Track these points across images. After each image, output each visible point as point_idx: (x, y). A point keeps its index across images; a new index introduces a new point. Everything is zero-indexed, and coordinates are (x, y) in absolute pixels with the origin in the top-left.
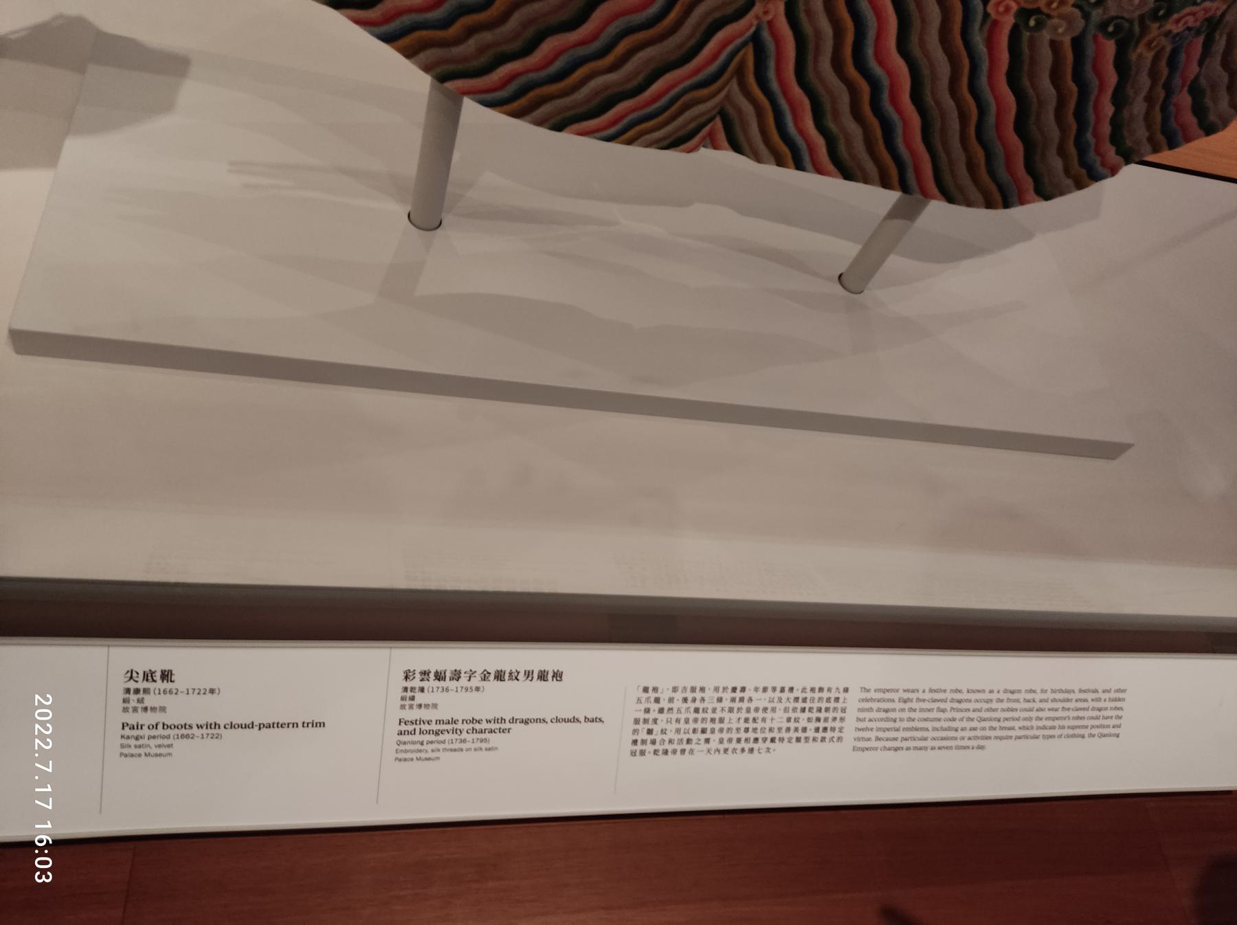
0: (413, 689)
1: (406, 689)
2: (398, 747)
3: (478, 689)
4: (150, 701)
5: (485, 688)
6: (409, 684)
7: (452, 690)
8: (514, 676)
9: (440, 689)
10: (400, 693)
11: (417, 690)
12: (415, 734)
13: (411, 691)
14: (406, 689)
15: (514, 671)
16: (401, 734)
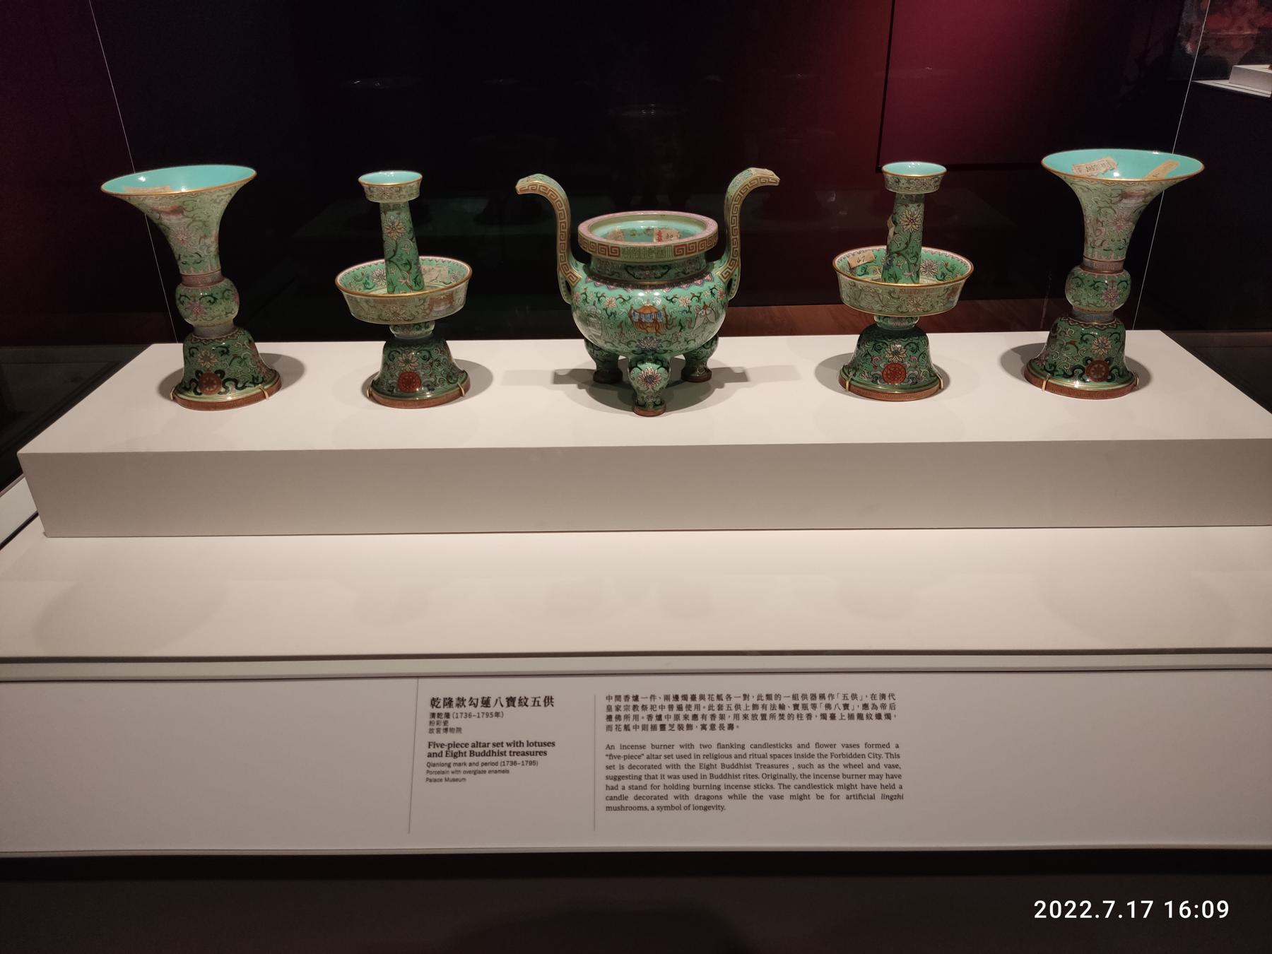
0: (439, 715)
1: (433, 715)
2: (428, 769)
3: (497, 714)
4: (452, 723)
5: (504, 713)
6: (436, 710)
7: (474, 716)
8: (523, 702)
9: (464, 715)
10: (428, 719)
12: (442, 756)
13: (438, 717)
14: (433, 715)
15: (523, 697)
16: (431, 756)
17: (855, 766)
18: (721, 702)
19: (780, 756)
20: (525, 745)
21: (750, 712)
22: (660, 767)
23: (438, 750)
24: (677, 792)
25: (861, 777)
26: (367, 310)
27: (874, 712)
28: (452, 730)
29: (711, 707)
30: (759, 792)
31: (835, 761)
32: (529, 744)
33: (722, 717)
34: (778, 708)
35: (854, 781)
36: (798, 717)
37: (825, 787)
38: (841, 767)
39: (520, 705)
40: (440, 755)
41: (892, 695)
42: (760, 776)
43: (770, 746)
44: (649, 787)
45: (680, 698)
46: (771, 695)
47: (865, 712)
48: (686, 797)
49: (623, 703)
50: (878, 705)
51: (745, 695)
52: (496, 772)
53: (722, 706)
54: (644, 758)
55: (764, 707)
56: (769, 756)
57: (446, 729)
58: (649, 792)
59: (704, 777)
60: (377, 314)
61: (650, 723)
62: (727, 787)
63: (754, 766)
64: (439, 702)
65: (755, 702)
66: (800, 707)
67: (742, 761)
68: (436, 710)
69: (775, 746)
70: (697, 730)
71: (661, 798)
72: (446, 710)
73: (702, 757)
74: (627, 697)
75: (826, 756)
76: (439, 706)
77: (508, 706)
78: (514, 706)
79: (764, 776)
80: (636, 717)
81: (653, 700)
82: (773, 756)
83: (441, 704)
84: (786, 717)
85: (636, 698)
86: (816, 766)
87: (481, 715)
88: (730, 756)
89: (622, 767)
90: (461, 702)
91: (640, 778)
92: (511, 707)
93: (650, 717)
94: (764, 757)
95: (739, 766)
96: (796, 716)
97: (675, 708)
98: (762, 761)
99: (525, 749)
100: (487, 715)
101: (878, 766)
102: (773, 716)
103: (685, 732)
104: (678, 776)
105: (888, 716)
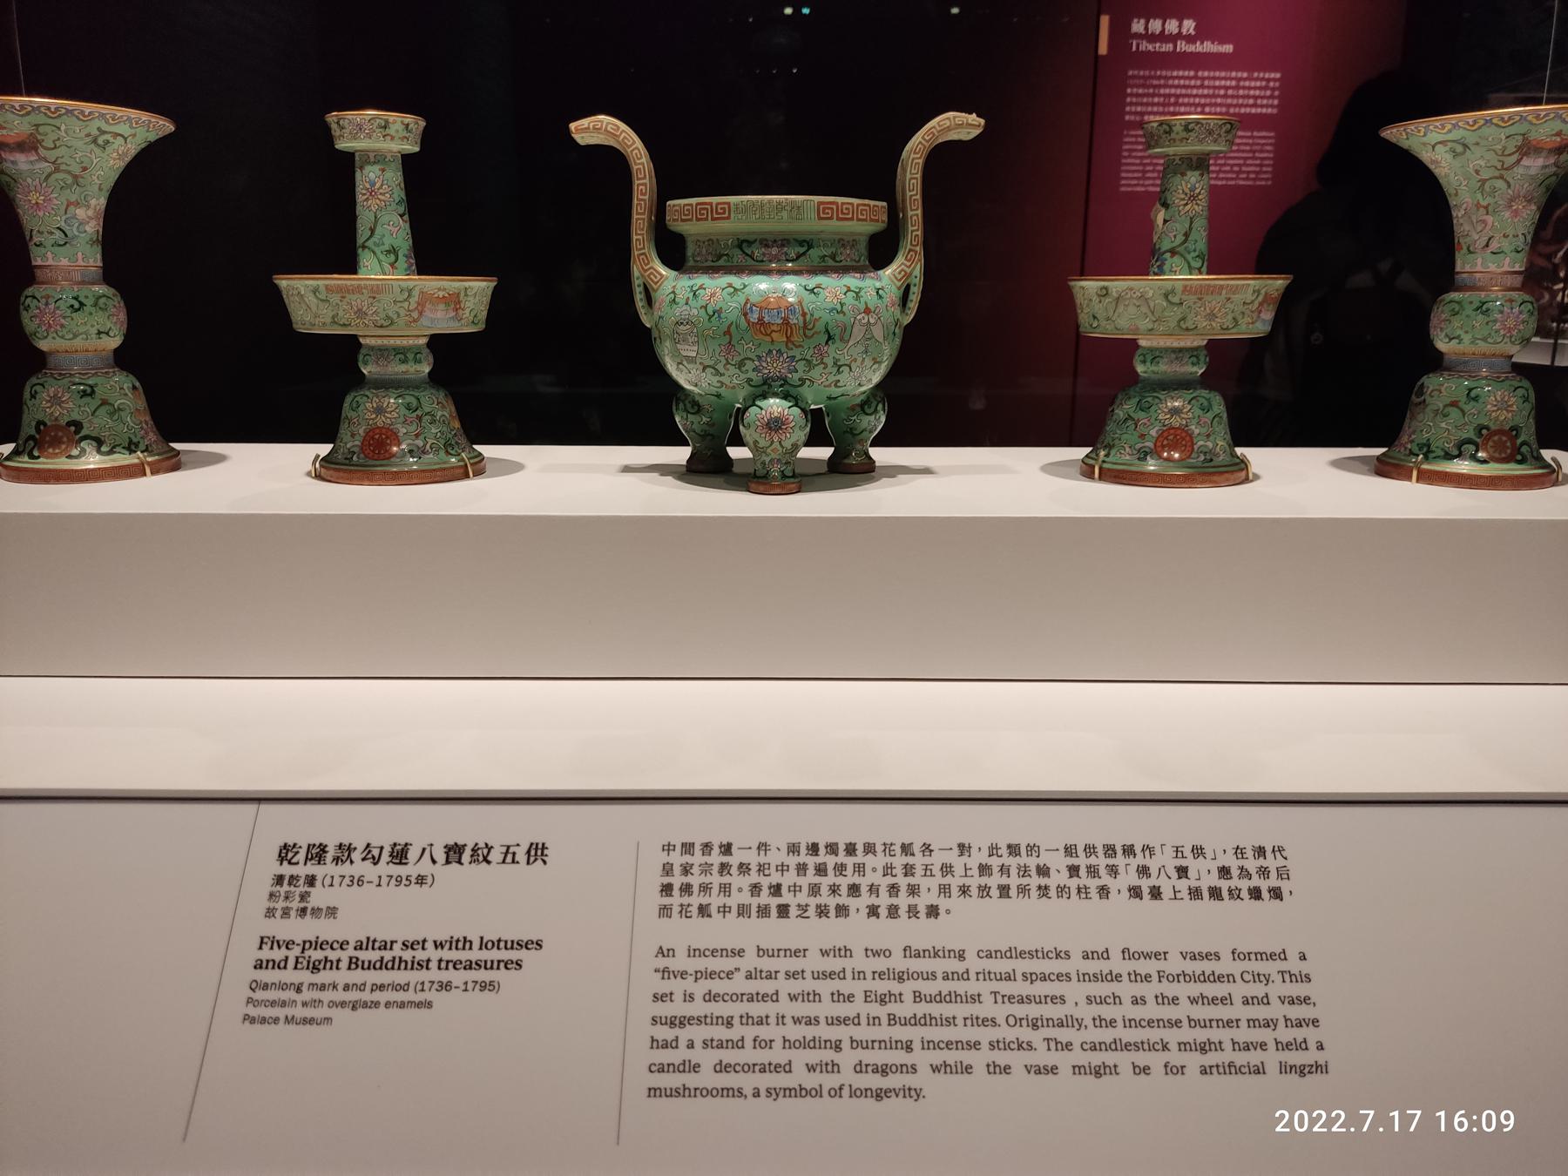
0: (293, 879)
6: (287, 870)
9: (347, 881)
10: (267, 886)
11: (302, 881)
13: (290, 884)
17: (1214, 1001)
18: (910, 860)
19: (1044, 978)
20: (476, 945)
21: (975, 881)
22: (775, 997)
23: (278, 954)
24: (814, 1056)
25: (1229, 1023)
26: (314, 309)
27: (1244, 885)
28: (316, 912)
29: (888, 870)
30: (1002, 1058)
31: (1170, 989)
32: (483, 945)
33: (913, 890)
34: (1033, 872)
35: (1215, 1034)
36: (1079, 892)
37: (1152, 1048)
38: (1184, 1001)
39: (474, 859)
40: (281, 965)
41: (1278, 850)
42: (1001, 1020)
43: (1021, 955)
44: (749, 1043)
45: (822, 850)
46: (1018, 846)
47: (1224, 885)
48: (833, 1067)
49: (697, 859)
50: (1253, 871)
51: (961, 847)
52: (402, 1005)
53: (912, 867)
54: (739, 977)
55: (1004, 870)
56: (1019, 977)
57: (304, 910)
58: (749, 1055)
59: (874, 1021)
60: (331, 314)
61: (755, 902)
62: (928, 1045)
63: (988, 999)
64: (297, 853)
65: (985, 860)
66: (1083, 872)
67: (960, 987)
68: (287, 870)
69: (1033, 954)
70: (858, 919)
71: (777, 1068)
72: (311, 869)
73: (869, 976)
74: (707, 847)
75: (1147, 978)
76: (294, 861)
77: (448, 862)
78: (460, 862)
79: (1011, 1020)
80: (725, 889)
81: (762, 853)
82: (1030, 977)
83: (301, 857)
84: (1053, 893)
85: (727, 849)
86: (1127, 1000)
87: (385, 880)
88: (932, 976)
89: (689, 998)
90: (345, 852)
91: (729, 1023)
92: (455, 866)
93: (755, 889)
94: (1009, 977)
95: (953, 998)
96: (1074, 892)
97: (811, 871)
98: (1006, 988)
99: (475, 955)
100: (399, 880)
101: (1265, 1000)
102: (1023, 890)
103: (832, 921)
104: (817, 1020)
105: (1276, 894)
